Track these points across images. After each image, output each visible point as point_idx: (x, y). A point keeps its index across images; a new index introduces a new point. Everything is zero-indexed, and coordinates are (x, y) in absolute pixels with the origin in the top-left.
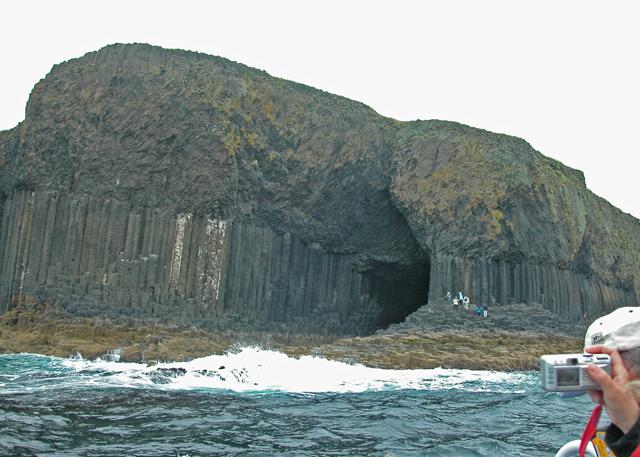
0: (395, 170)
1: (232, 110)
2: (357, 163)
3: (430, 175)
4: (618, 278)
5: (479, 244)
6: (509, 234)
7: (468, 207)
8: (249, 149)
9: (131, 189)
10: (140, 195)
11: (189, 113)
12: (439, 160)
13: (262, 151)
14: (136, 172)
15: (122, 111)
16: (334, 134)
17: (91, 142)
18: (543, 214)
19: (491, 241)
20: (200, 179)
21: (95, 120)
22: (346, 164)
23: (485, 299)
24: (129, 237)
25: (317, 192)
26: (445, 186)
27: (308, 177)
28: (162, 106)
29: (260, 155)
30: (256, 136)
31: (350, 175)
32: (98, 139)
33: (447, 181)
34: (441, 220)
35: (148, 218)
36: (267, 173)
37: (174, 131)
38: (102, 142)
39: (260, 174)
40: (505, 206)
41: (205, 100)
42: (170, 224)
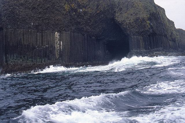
2: (104, 11)
4: (173, 39)
5: (143, 32)
6: (152, 27)
7: (140, 21)
8: (72, 9)
10: (40, 27)
13: (76, 9)
17: (22, 12)
18: (159, 21)
24: (38, 41)
25: (93, 21)
26: (132, 15)
27: (90, 16)
29: (76, 11)
30: (74, 5)
31: (102, 14)
35: (44, 34)
36: (78, 16)
38: (25, 12)
39: (76, 17)
40: (150, 19)
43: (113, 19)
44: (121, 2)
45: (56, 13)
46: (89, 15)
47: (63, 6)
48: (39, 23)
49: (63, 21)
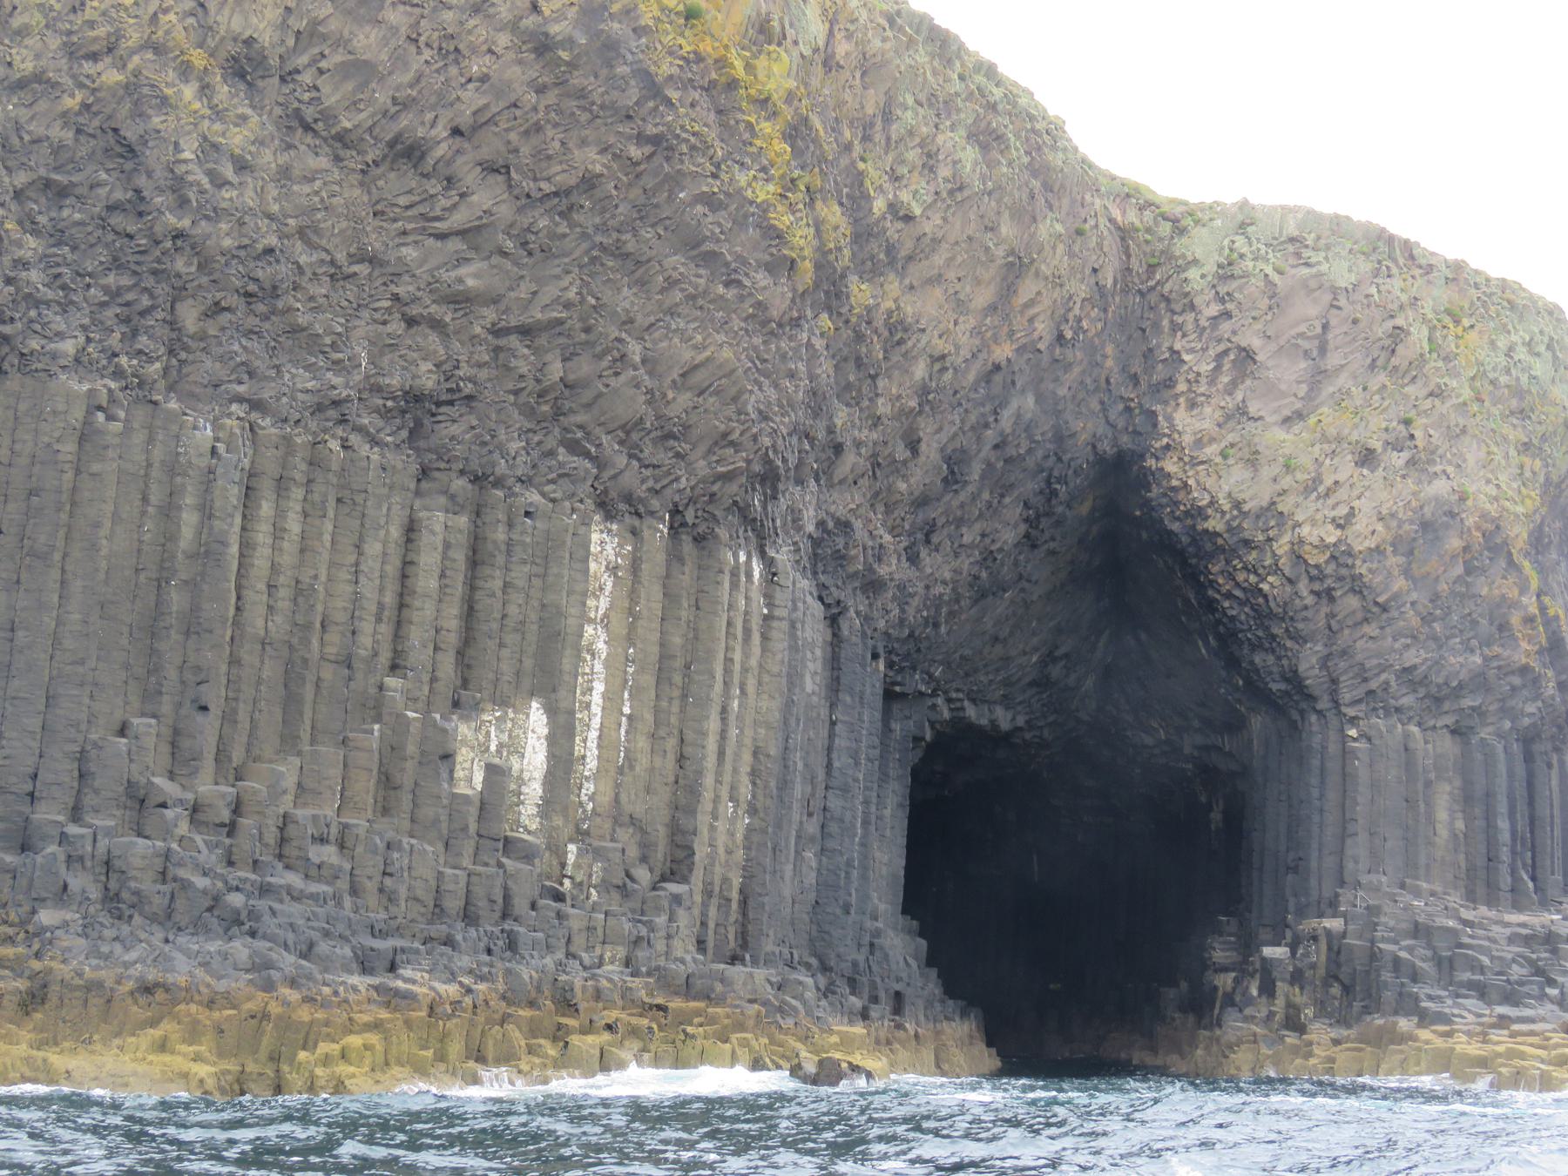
0: (1169, 383)
1: (790, 97)
3: (1300, 416)
5: (1479, 681)
7: (1454, 543)
9: (414, 397)
10: (455, 429)
11: (653, 89)
12: (1333, 360)
14: (436, 325)
15: (367, 41)
16: (1007, 229)
17: (242, 166)
19: (1524, 670)
20: (699, 378)
21: (245, 66)
22: (1020, 350)
23: (1505, 881)
25: (930, 450)
27: (924, 391)
28: (543, 46)
32: (268, 158)
33: (1377, 445)
34: (1357, 587)
37: (593, 160)
38: (284, 173)
41: (707, 47)
42: (559, 557)
43: (1122, 477)
44: (1257, 282)
45: (671, 283)
46: (920, 370)
47: (765, 208)
48: (447, 369)
49: (751, 404)
